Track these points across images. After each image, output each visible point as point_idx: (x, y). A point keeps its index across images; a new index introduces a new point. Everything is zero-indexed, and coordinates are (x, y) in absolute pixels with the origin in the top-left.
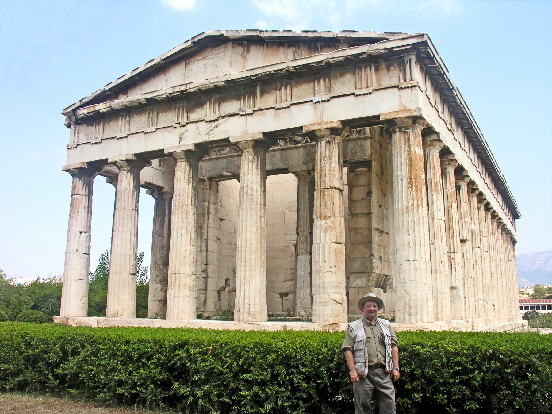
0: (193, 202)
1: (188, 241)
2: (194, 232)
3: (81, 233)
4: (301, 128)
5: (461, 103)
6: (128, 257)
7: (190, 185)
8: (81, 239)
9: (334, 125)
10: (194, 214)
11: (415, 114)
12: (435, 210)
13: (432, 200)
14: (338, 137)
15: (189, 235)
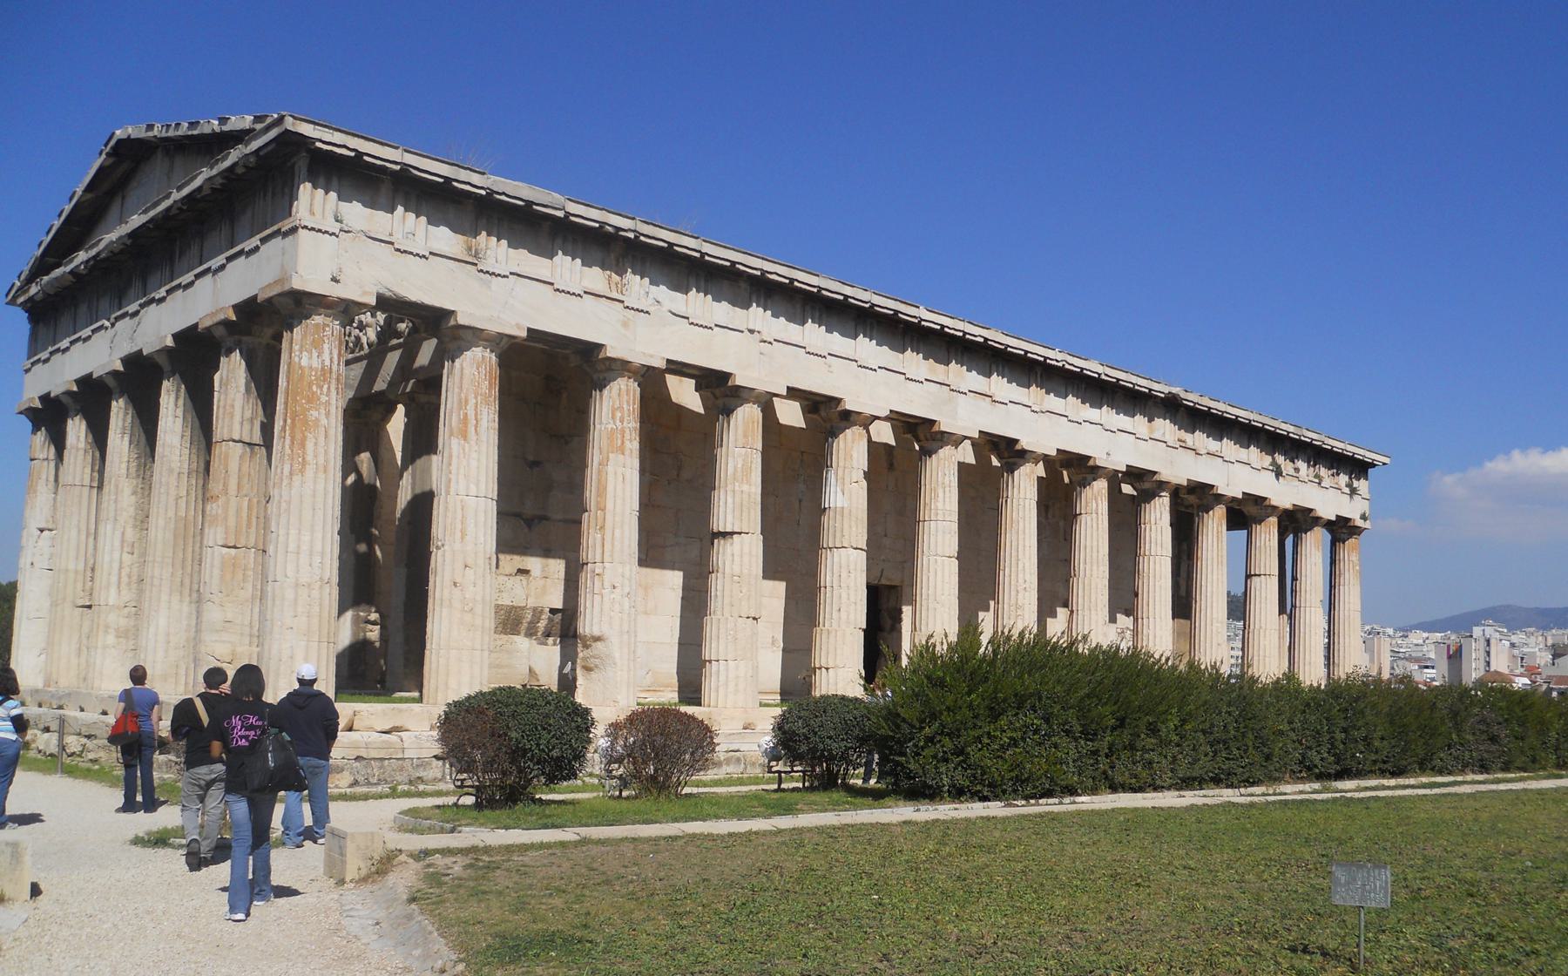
0: (133, 470)
1: (117, 543)
2: (135, 526)
3: (42, 531)
4: (196, 325)
5: (619, 229)
6: (72, 575)
7: (127, 438)
8: (40, 543)
9: (222, 317)
10: (134, 493)
11: (286, 288)
12: (453, 477)
13: (451, 456)
14: (245, 339)
15: (118, 534)
